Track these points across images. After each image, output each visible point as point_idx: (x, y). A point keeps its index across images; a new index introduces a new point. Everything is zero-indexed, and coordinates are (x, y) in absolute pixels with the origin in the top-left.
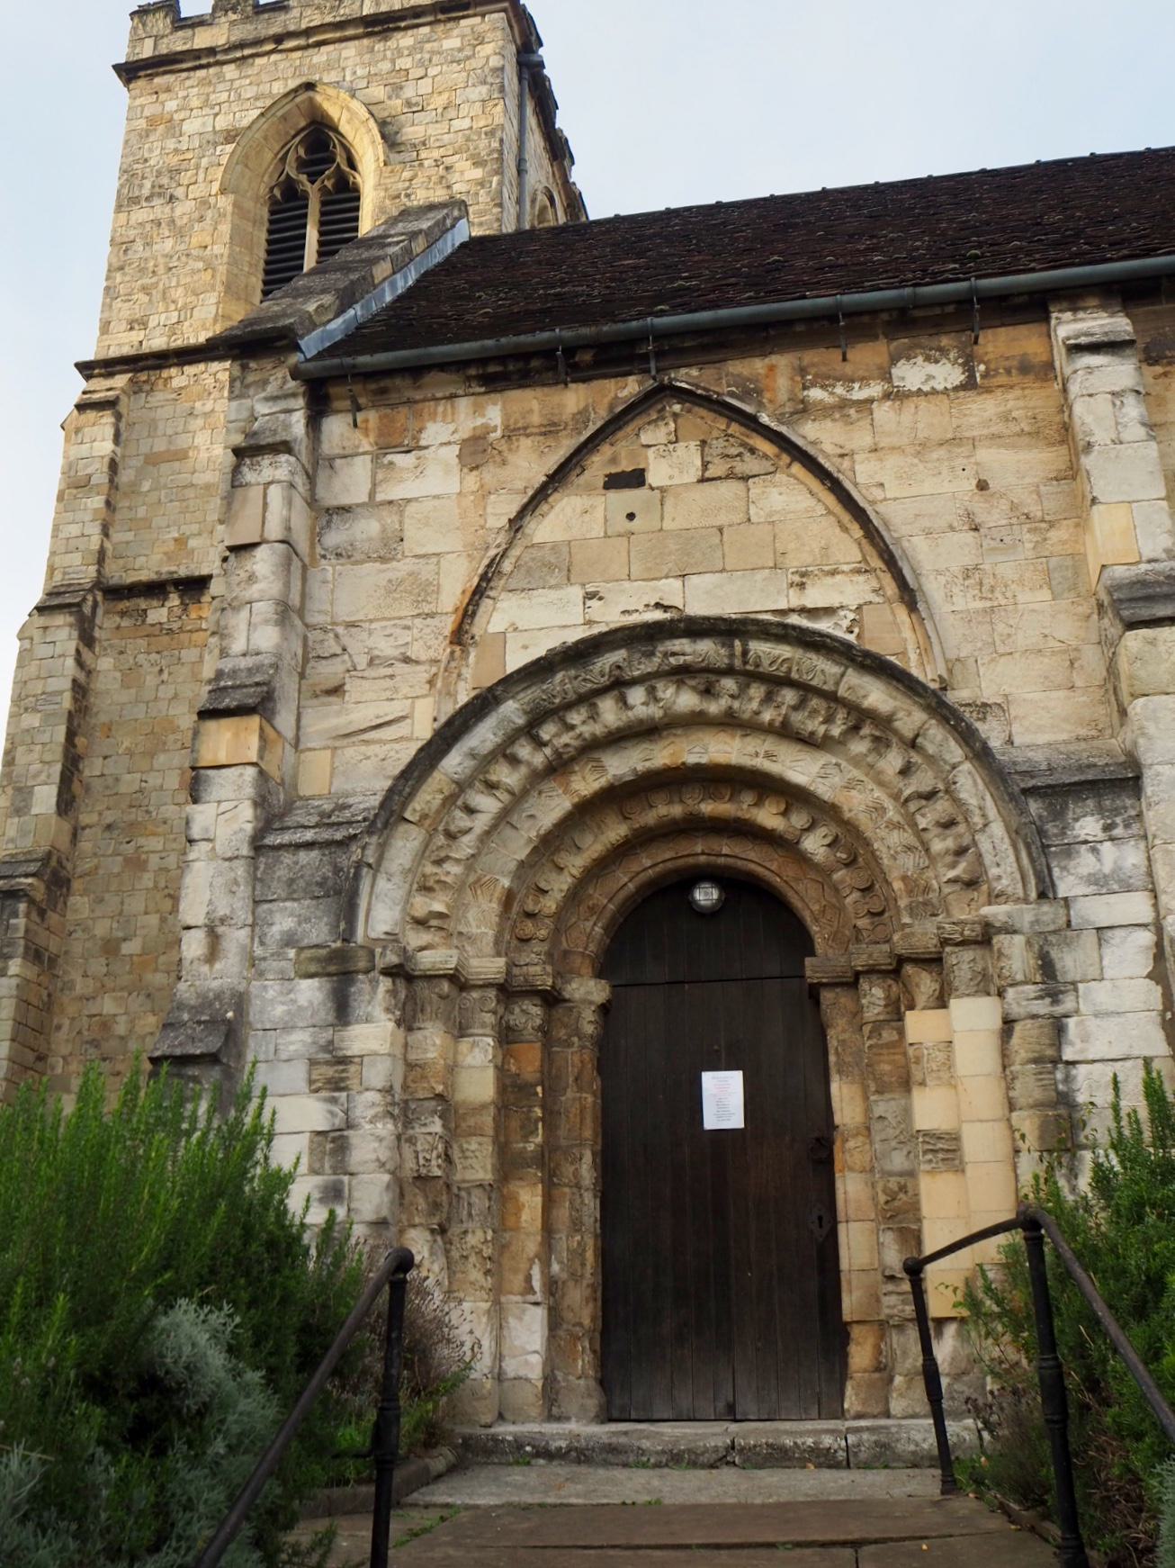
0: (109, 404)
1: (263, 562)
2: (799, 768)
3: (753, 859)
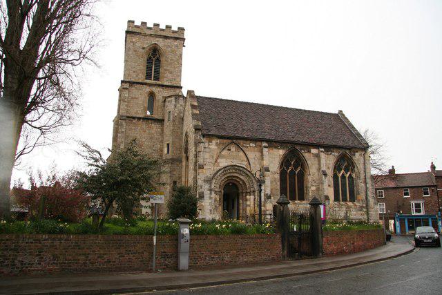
0: (127, 89)
1: (201, 153)
2: (241, 177)
3: (236, 182)
